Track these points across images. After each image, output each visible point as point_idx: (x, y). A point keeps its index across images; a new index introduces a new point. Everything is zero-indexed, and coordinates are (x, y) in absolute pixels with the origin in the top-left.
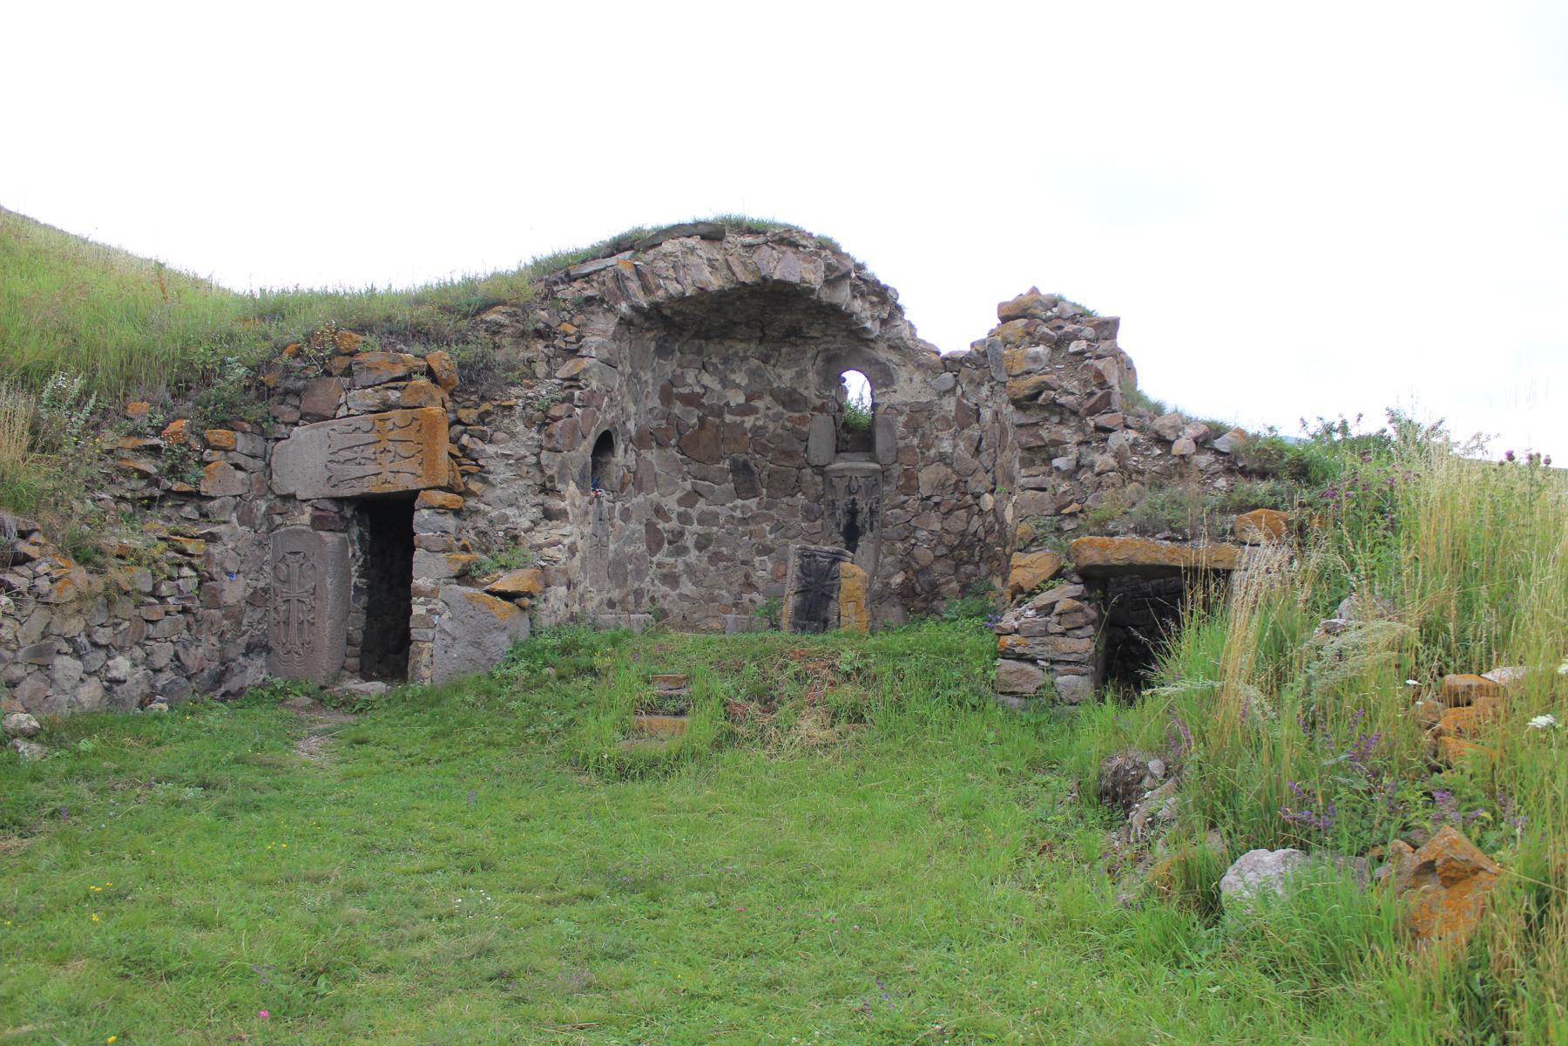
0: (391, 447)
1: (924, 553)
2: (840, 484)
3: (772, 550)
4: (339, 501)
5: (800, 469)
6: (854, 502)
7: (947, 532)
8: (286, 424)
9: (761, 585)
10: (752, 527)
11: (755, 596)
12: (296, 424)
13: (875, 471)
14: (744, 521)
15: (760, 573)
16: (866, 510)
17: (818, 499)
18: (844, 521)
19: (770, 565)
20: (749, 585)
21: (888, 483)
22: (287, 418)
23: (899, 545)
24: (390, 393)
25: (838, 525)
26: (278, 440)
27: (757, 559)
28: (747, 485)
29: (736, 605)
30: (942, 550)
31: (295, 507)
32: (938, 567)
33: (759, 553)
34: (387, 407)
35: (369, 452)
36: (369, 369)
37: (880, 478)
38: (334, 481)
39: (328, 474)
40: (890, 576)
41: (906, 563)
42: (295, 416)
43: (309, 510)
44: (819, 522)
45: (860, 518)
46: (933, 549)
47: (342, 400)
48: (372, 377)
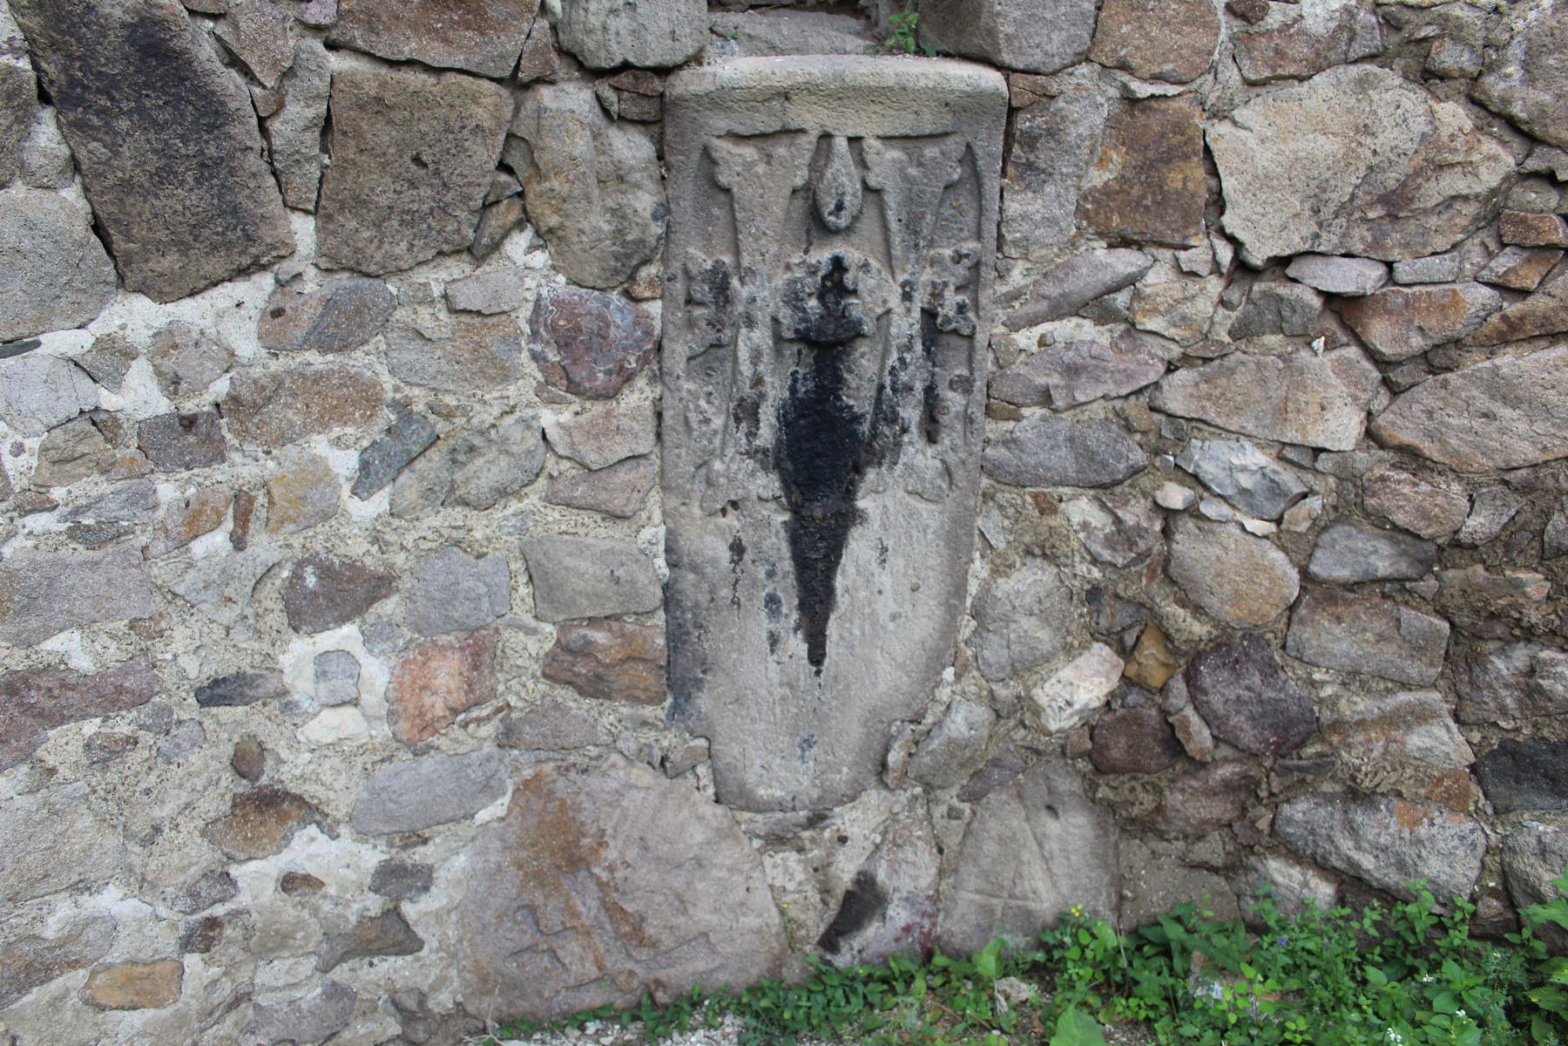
1: (1240, 564)
2: (764, 182)
3: (382, 585)
5: (517, 84)
6: (835, 282)
7: (1411, 458)
9: (338, 789)
10: (244, 466)
11: (308, 849)
13: (968, 106)
14: (187, 436)
15: (326, 726)
16: (906, 324)
17: (625, 268)
18: (776, 391)
19: (377, 673)
20: (266, 806)
21: (1032, 175)
23: (1082, 510)
25: (746, 412)
27: (298, 655)
28: (186, 198)
29: (203, 937)
30: (1360, 553)
32: (1336, 640)
33: (303, 613)
37: (990, 145)
40: (1028, 666)
41: (1116, 612)
44: (638, 397)
45: (864, 371)
46: (1301, 548)
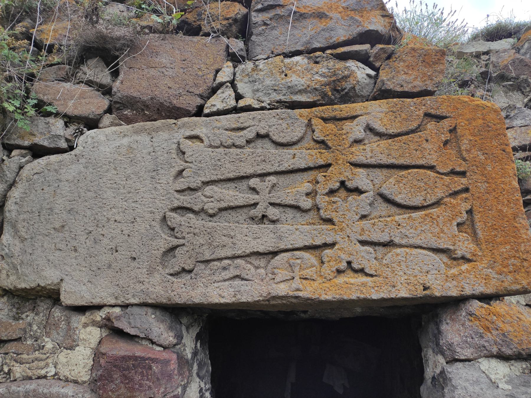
0: (361, 179)
4: (174, 312)
8: (69, 120)
12: (92, 123)
22: (71, 109)
24: (352, 64)
26: (37, 152)
31: (48, 326)
34: (342, 93)
35: (296, 190)
36: (300, 16)
38: (181, 259)
39: (165, 240)
42: (96, 104)
43: (90, 335)
47: (224, 76)
48: (308, 33)
